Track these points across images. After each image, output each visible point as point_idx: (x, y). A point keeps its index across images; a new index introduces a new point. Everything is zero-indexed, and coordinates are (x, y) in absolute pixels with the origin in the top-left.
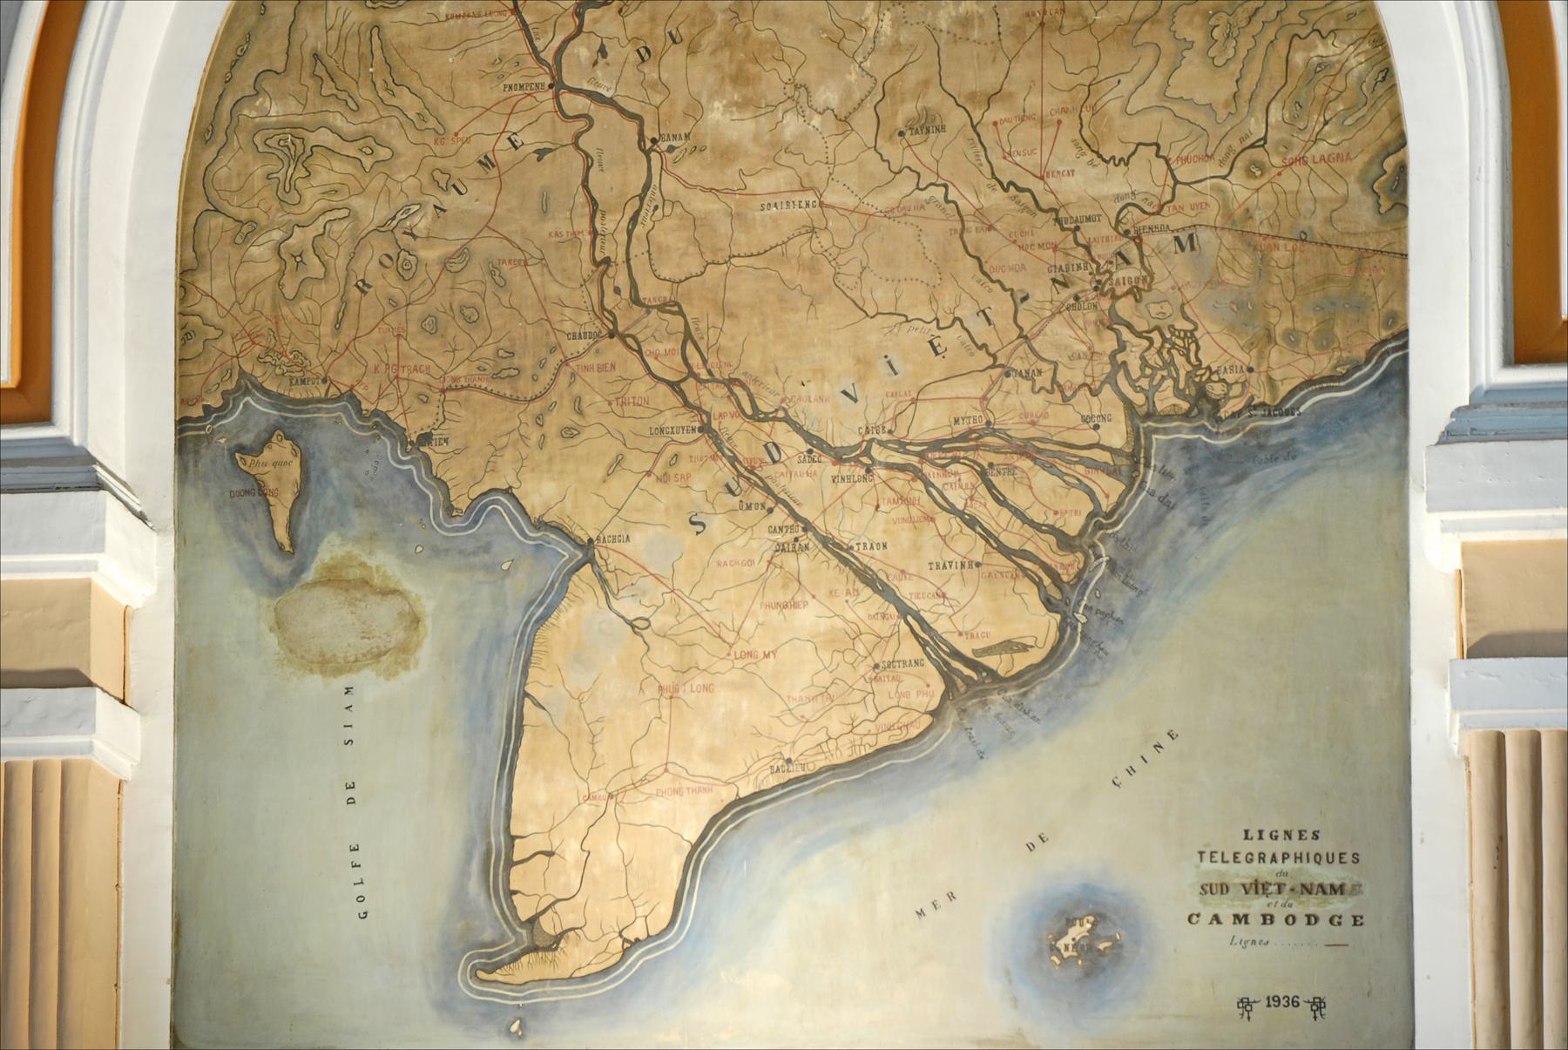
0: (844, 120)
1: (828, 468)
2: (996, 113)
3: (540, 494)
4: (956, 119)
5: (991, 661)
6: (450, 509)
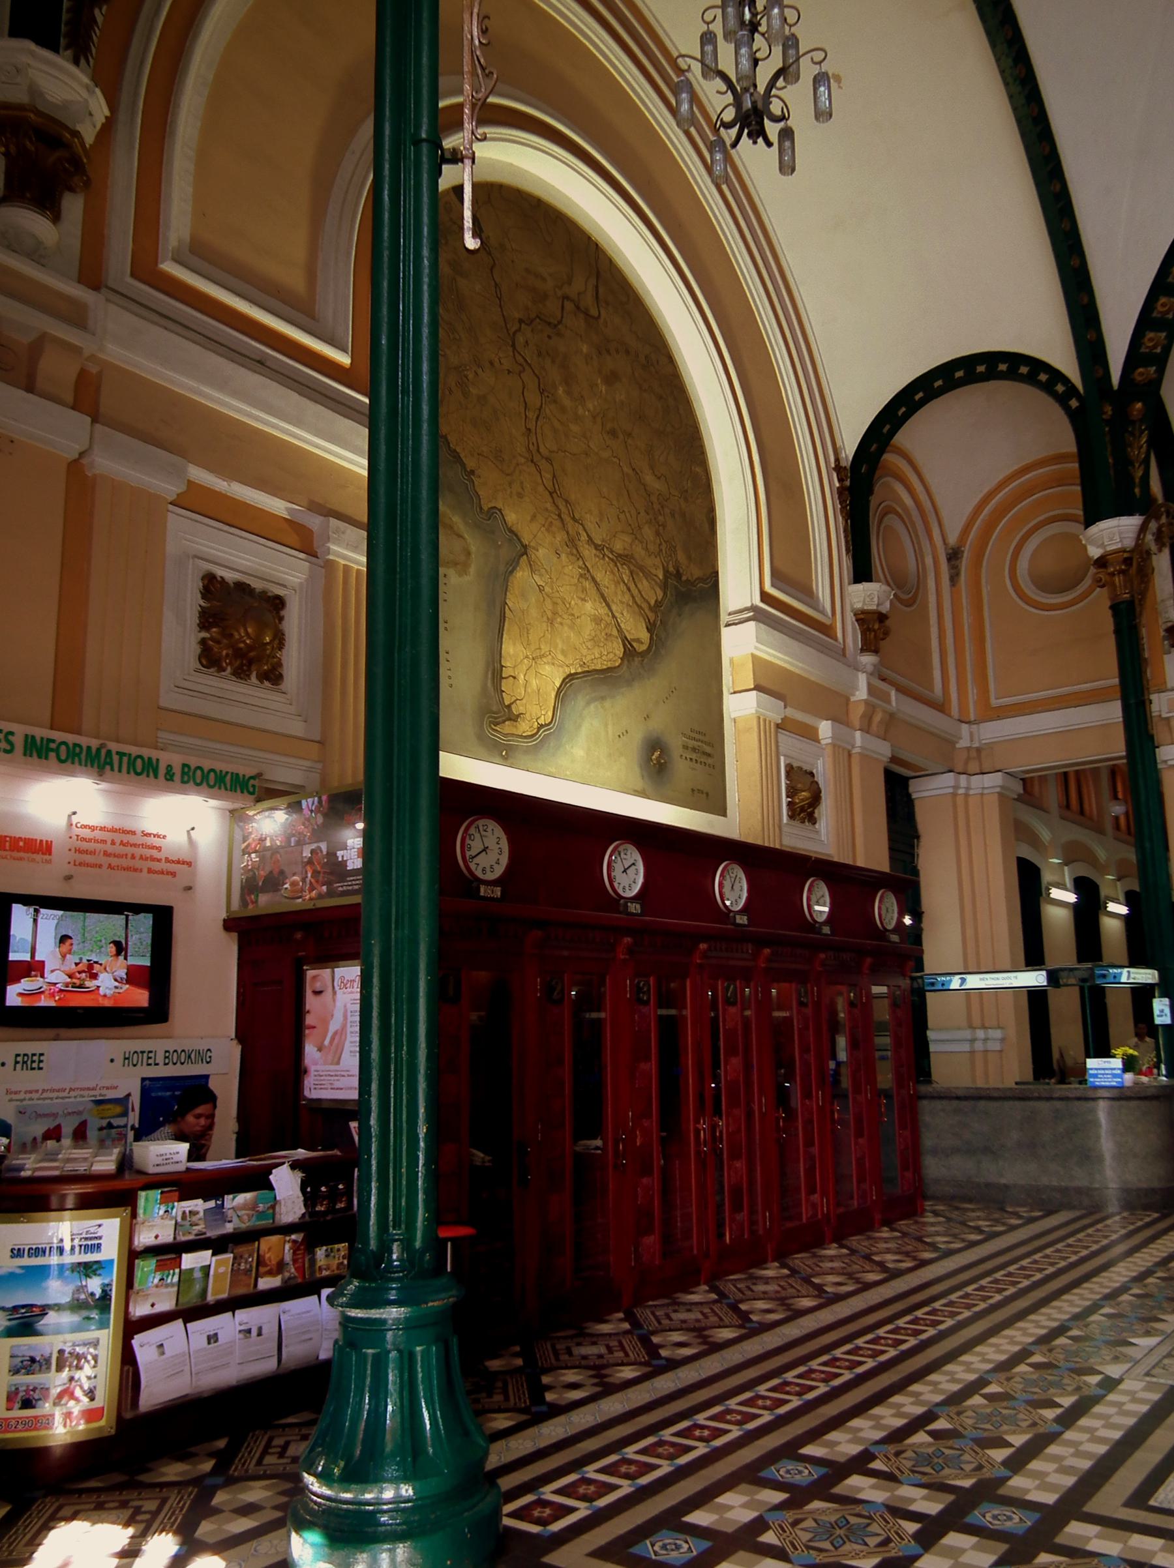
0: (594, 417)
1: (594, 551)
2: (629, 441)
3: (511, 517)
4: (621, 436)
5: (635, 644)
6: (481, 508)
